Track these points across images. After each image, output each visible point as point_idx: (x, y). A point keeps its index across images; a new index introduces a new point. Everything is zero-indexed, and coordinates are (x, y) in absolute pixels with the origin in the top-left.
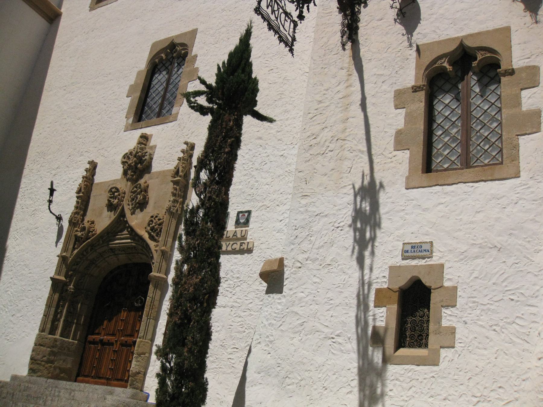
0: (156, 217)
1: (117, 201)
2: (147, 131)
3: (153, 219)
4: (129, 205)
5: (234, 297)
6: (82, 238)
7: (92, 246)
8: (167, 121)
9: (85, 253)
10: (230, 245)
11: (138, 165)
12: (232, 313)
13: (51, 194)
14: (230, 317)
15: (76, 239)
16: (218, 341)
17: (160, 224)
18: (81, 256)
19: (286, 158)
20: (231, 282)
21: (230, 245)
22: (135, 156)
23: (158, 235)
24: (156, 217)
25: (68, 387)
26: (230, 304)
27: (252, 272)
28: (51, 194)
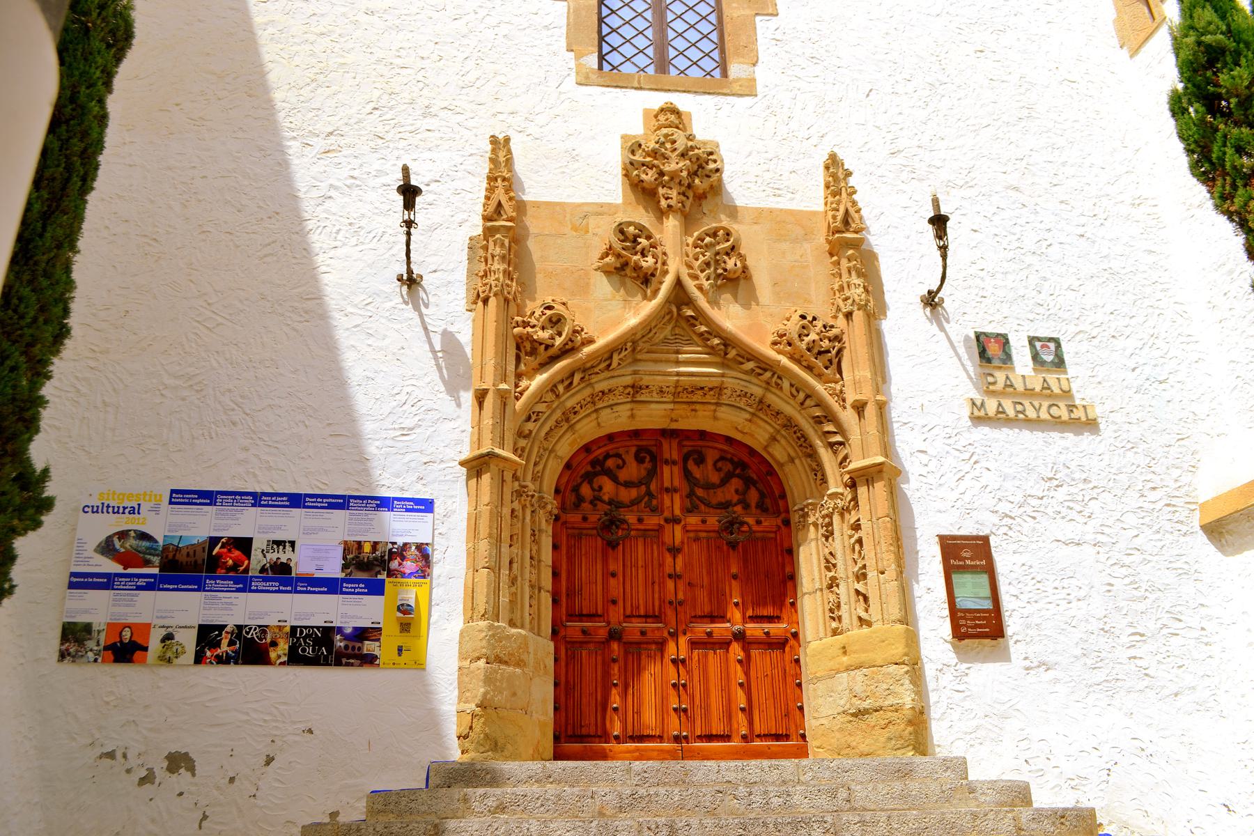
0: (814, 319)
1: (650, 260)
2: (683, 101)
3: (805, 322)
4: (696, 277)
5: (1092, 523)
6: (547, 347)
7: (586, 370)
8: (725, 91)
9: (561, 388)
10: (1044, 409)
11: (676, 179)
12: (1102, 557)
13: (409, 205)
14: (1101, 567)
15: (518, 348)
16: (1091, 620)
17: (837, 338)
18: (550, 397)
19: (1094, 242)
20: (1073, 490)
21: (1044, 409)
22: (683, 155)
23: (836, 364)
24: (814, 319)
25: (731, 776)
26: (1089, 537)
27: (1113, 471)
28: (409, 205)
